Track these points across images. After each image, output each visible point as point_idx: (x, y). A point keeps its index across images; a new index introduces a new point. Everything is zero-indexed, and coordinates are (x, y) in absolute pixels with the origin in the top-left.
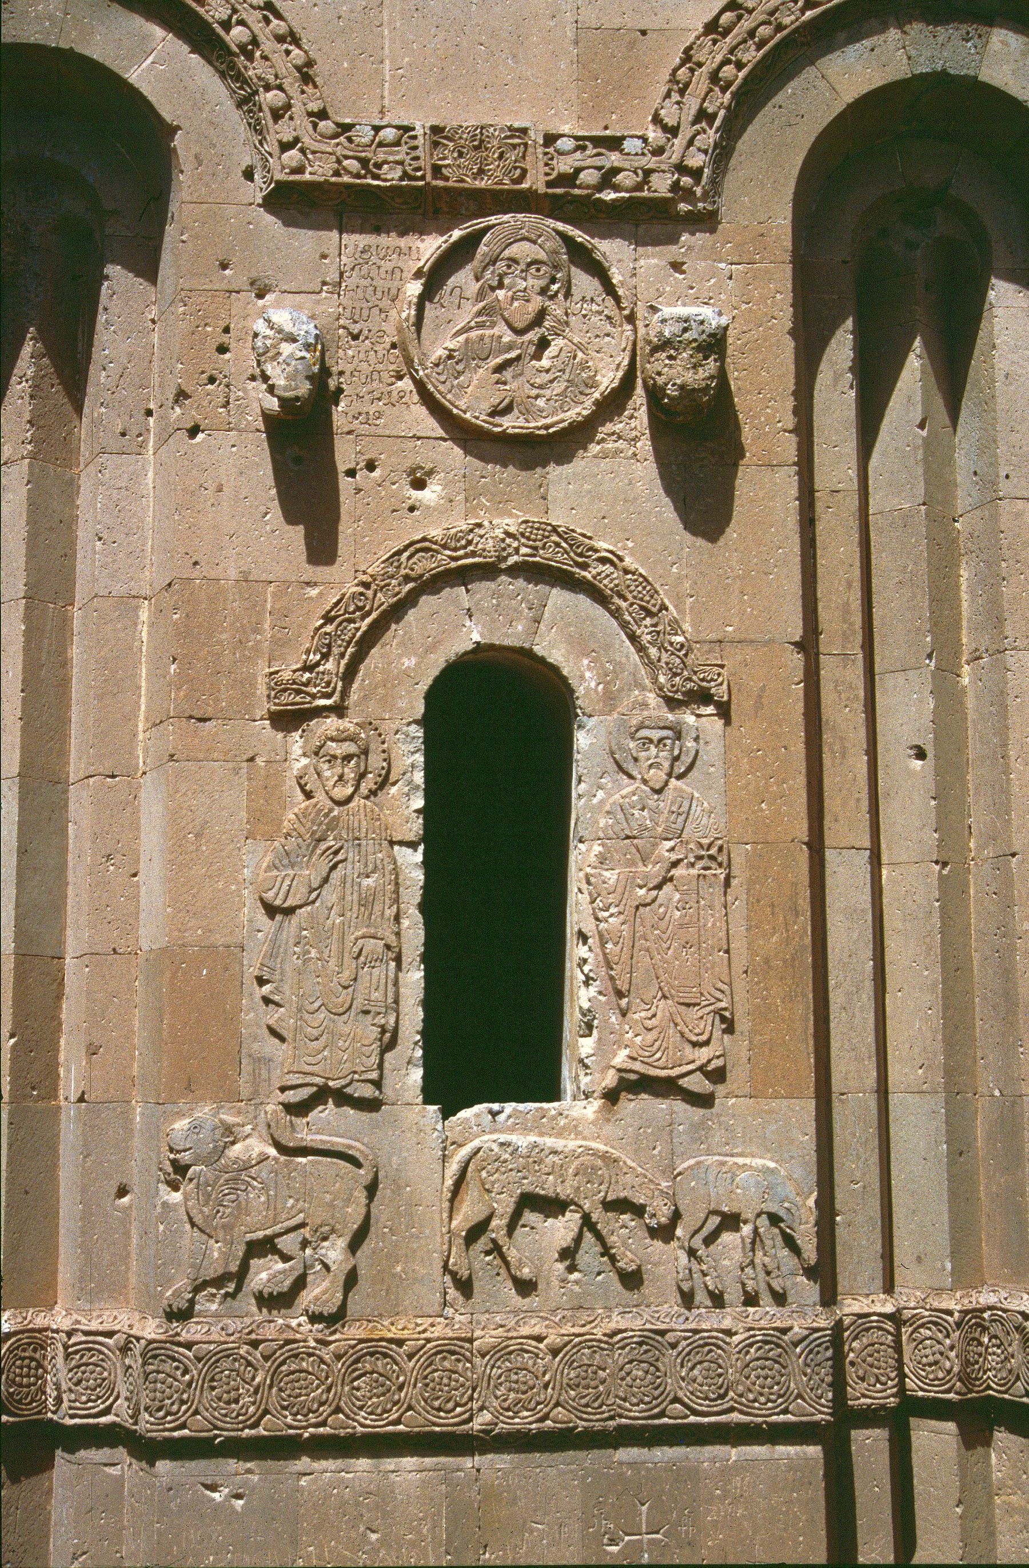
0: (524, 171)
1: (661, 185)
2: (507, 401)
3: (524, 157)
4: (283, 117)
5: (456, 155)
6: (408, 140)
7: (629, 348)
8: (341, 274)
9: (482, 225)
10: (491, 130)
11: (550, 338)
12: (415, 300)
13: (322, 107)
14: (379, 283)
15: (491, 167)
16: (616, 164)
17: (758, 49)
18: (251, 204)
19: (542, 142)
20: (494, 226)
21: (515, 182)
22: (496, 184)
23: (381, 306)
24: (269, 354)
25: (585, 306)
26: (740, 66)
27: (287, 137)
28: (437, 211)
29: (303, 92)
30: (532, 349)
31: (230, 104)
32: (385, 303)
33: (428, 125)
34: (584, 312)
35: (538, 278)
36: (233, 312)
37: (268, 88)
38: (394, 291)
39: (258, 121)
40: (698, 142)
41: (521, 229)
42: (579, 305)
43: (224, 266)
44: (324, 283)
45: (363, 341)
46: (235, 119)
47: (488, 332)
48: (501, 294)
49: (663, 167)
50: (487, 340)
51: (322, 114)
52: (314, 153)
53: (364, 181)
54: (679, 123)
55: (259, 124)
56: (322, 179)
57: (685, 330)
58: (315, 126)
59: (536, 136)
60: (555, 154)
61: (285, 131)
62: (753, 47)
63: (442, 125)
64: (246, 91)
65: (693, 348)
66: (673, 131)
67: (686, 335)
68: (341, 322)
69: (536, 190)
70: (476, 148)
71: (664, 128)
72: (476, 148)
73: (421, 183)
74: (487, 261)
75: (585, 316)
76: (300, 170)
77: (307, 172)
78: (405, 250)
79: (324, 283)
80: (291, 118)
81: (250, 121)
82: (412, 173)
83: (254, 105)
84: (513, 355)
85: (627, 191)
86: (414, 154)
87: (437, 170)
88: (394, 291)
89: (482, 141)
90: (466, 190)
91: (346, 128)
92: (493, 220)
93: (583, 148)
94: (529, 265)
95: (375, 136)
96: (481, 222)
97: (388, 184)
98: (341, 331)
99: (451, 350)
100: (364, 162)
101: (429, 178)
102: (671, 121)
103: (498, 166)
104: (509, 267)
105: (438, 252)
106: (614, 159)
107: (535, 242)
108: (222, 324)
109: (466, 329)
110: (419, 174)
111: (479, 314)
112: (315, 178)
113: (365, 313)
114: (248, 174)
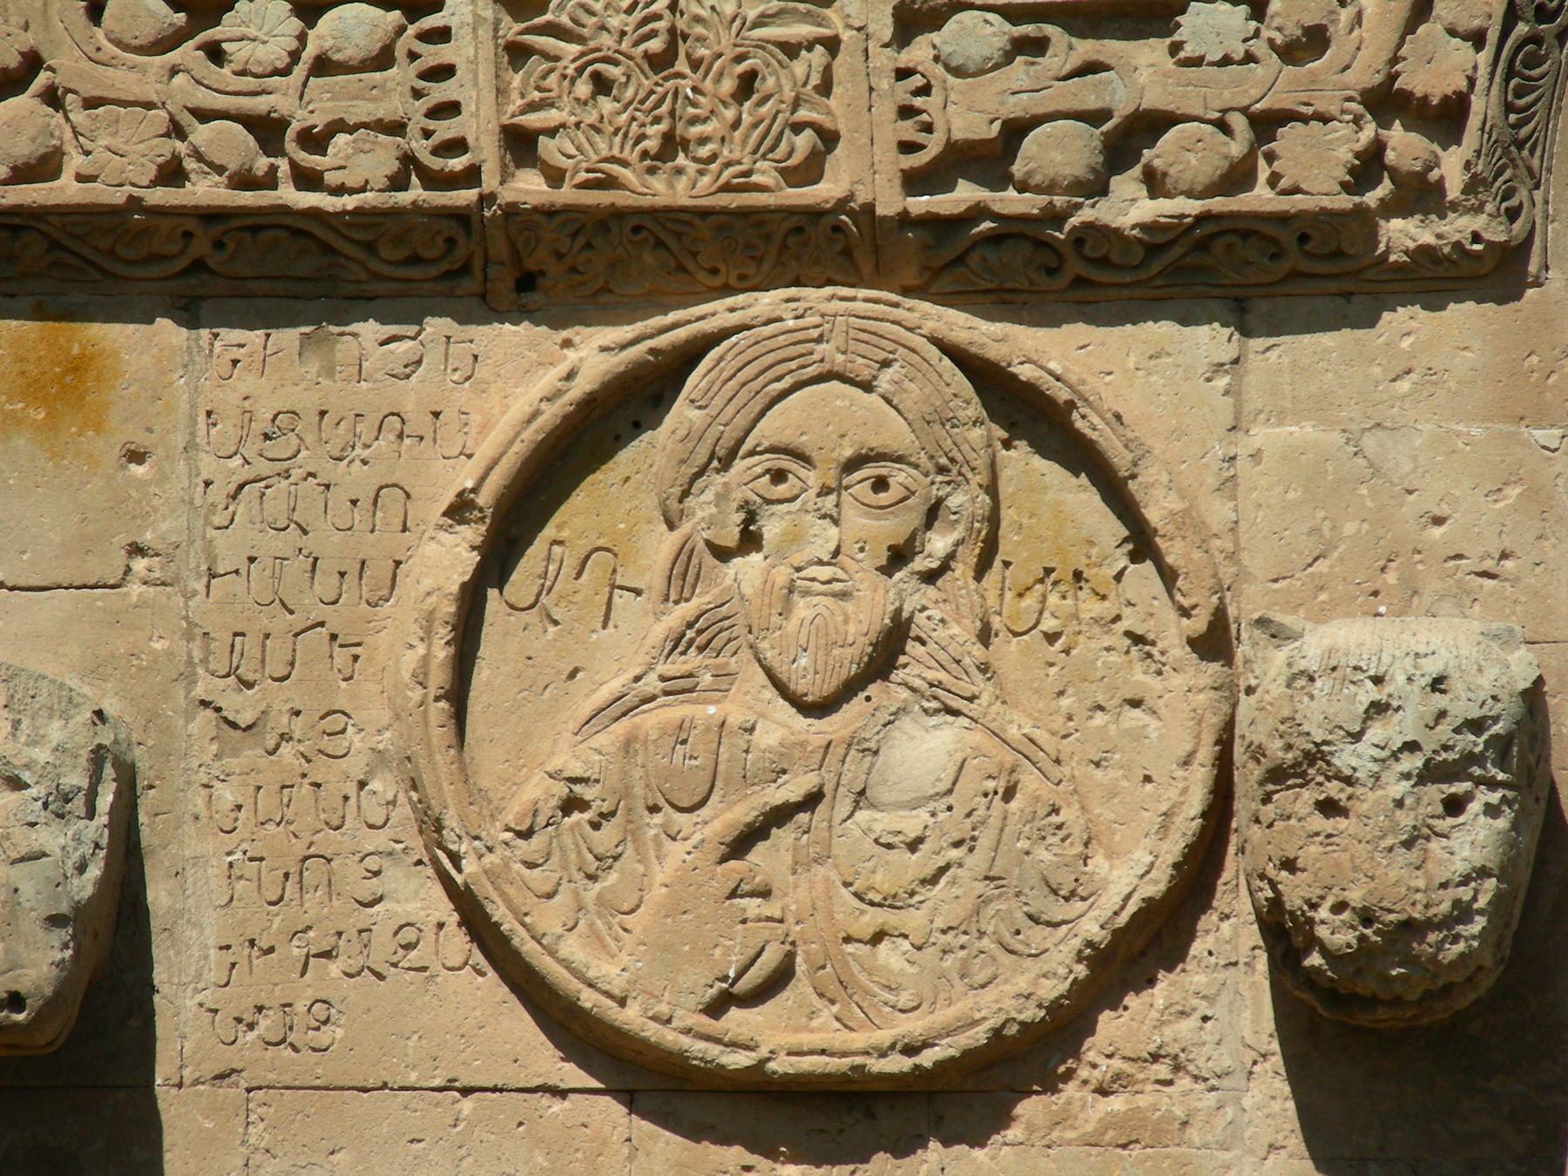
0: (829, 139)
2: (770, 959)
3: (825, 88)
5: (583, 88)
6: (419, 47)
7: (1207, 752)
9: (681, 334)
14: (327, 541)
16: (1155, 100)
19: (887, 33)
22: (727, 188)
25: (1053, 599)
28: (526, 282)
34: (1049, 624)
41: (819, 340)
42: (1030, 601)
44: (137, 550)
52: (91, 103)
56: (118, 197)
65: (1406, 776)
69: (869, 208)
70: (660, 62)
74: (701, 456)
75: (1051, 638)
76: (45, 167)
78: (418, 421)
79: (137, 550)
82: (436, 163)
84: (791, 790)
85: (1190, 194)
86: (441, 92)
88: (379, 570)
92: (717, 313)
93: (1037, 46)
95: (302, 38)
97: (349, 202)
100: (267, 130)
103: (736, 124)
107: (867, 387)
110: (457, 164)
111: (677, 643)
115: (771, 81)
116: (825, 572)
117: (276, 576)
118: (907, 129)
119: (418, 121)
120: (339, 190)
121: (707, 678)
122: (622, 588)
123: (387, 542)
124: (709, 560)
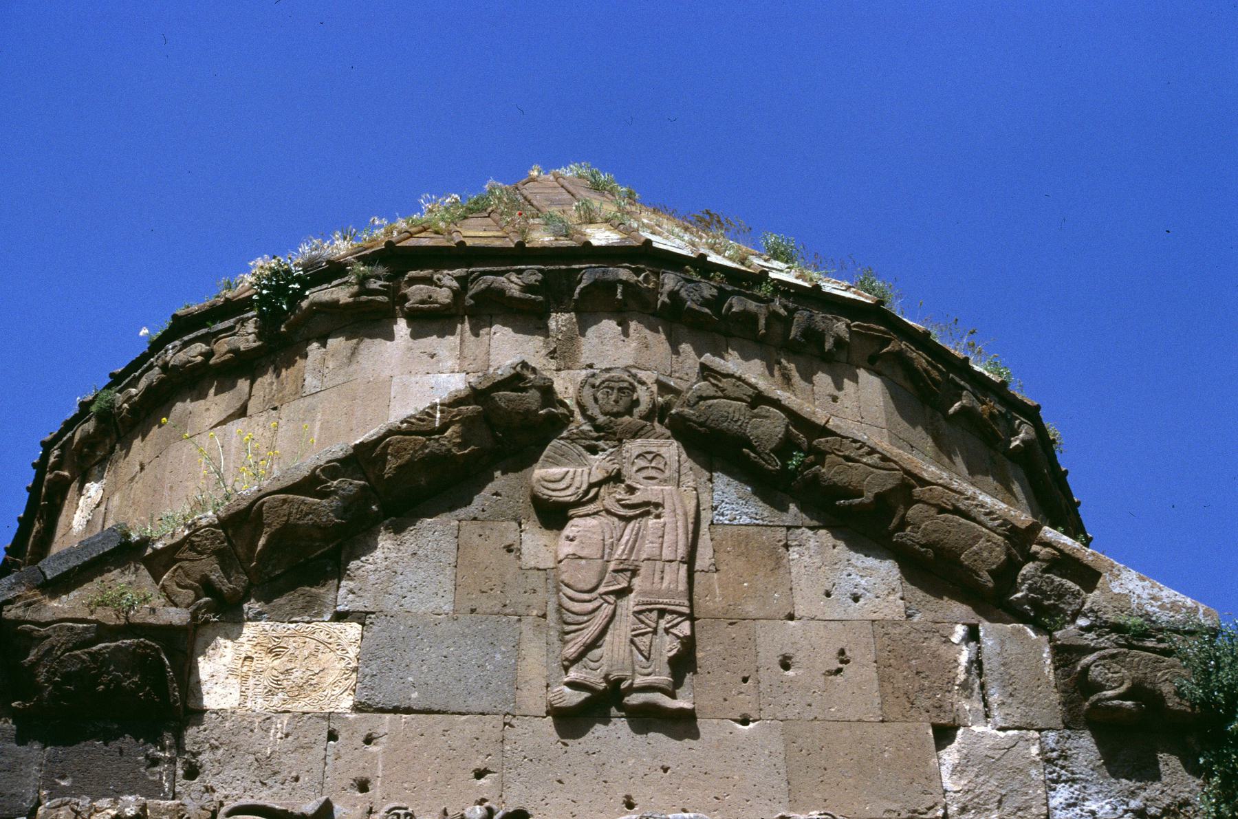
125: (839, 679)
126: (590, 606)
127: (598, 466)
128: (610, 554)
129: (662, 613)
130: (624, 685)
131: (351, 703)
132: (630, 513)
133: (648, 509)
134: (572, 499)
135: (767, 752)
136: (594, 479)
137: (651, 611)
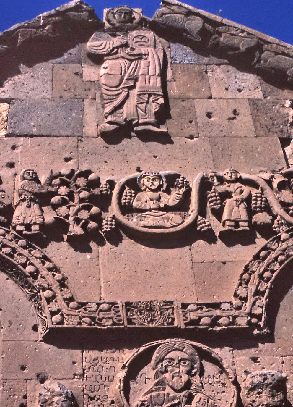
0: (173, 319)
1: (242, 322)
3: (173, 313)
4: (52, 301)
5: (138, 314)
6: (115, 308)
8: (84, 370)
9: (154, 344)
10: (156, 302)
11: (194, 394)
12: (122, 379)
13: (71, 296)
14: (103, 374)
15: (157, 318)
16: (218, 314)
17: (280, 265)
18: (36, 341)
19: (181, 307)
20: (161, 344)
21: (168, 324)
22: (160, 325)
23: (105, 384)
24: (48, 403)
25: (210, 379)
26: (273, 271)
27: (54, 309)
29: (61, 291)
30: (185, 399)
31: (25, 300)
32: (107, 383)
33: (124, 302)
34: (210, 382)
35: (185, 367)
36: (28, 388)
37: (44, 290)
38: (111, 377)
39: (40, 304)
40: (257, 303)
41: (175, 345)
42: (207, 379)
43: (23, 368)
44: (75, 375)
45: (97, 401)
46: (29, 306)
47: (162, 392)
48: (166, 375)
49: (242, 314)
50: (161, 396)
51: (71, 299)
52: (68, 315)
53: (93, 327)
54: (247, 296)
55: (40, 305)
56: (72, 326)
57: (265, 379)
58: (68, 304)
59: (177, 304)
60: (188, 312)
61: (54, 307)
62: (278, 264)
63: (131, 302)
64: (34, 292)
65: (270, 387)
66: (245, 299)
67: (266, 382)
68: (85, 392)
69: (180, 327)
71: (241, 299)
72: (148, 310)
73: (122, 326)
74: (158, 360)
75: (211, 384)
76: (62, 322)
77: (65, 324)
78: (116, 358)
79: (75, 375)
80: (56, 301)
81: (36, 305)
82: (118, 322)
83: (38, 298)
84: (176, 401)
85: (225, 325)
86: (118, 314)
87: (130, 321)
88: (111, 377)
89: (151, 307)
90: (144, 328)
91: (83, 304)
92: (160, 342)
93: (202, 308)
94: (180, 361)
95: (98, 308)
96: (154, 343)
97: (106, 327)
98: (85, 396)
99: (143, 401)
100: (93, 319)
101: (126, 324)
102: (243, 295)
103: (161, 318)
104: (170, 362)
105: (133, 357)
106: (218, 312)
107: (182, 351)
108: (22, 394)
109: (150, 391)
110: (121, 322)
111: (156, 384)
112: (69, 326)
113: (97, 388)
114: (35, 328)
115: (165, 313)
116: (178, 374)
117: (96, 378)
118: (184, 318)
119: (115, 317)
120: (104, 326)
121: (161, 389)
122: (148, 378)
123: (112, 373)
124: (160, 374)
125: (235, 121)
126: (116, 93)
127: (117, 41)
128: (125, 73)
129: (150, 95)
130: (134, 122)
131: (5, 133)
132: (133, 58)
133: (140, 57)
134: (106, 53)
135: (203, 149)
136: (115, 46)
137: (145, 94)
